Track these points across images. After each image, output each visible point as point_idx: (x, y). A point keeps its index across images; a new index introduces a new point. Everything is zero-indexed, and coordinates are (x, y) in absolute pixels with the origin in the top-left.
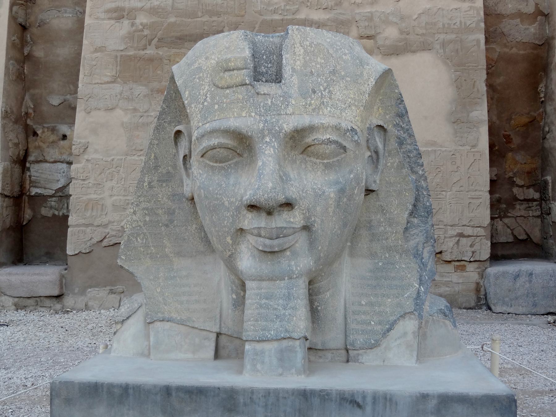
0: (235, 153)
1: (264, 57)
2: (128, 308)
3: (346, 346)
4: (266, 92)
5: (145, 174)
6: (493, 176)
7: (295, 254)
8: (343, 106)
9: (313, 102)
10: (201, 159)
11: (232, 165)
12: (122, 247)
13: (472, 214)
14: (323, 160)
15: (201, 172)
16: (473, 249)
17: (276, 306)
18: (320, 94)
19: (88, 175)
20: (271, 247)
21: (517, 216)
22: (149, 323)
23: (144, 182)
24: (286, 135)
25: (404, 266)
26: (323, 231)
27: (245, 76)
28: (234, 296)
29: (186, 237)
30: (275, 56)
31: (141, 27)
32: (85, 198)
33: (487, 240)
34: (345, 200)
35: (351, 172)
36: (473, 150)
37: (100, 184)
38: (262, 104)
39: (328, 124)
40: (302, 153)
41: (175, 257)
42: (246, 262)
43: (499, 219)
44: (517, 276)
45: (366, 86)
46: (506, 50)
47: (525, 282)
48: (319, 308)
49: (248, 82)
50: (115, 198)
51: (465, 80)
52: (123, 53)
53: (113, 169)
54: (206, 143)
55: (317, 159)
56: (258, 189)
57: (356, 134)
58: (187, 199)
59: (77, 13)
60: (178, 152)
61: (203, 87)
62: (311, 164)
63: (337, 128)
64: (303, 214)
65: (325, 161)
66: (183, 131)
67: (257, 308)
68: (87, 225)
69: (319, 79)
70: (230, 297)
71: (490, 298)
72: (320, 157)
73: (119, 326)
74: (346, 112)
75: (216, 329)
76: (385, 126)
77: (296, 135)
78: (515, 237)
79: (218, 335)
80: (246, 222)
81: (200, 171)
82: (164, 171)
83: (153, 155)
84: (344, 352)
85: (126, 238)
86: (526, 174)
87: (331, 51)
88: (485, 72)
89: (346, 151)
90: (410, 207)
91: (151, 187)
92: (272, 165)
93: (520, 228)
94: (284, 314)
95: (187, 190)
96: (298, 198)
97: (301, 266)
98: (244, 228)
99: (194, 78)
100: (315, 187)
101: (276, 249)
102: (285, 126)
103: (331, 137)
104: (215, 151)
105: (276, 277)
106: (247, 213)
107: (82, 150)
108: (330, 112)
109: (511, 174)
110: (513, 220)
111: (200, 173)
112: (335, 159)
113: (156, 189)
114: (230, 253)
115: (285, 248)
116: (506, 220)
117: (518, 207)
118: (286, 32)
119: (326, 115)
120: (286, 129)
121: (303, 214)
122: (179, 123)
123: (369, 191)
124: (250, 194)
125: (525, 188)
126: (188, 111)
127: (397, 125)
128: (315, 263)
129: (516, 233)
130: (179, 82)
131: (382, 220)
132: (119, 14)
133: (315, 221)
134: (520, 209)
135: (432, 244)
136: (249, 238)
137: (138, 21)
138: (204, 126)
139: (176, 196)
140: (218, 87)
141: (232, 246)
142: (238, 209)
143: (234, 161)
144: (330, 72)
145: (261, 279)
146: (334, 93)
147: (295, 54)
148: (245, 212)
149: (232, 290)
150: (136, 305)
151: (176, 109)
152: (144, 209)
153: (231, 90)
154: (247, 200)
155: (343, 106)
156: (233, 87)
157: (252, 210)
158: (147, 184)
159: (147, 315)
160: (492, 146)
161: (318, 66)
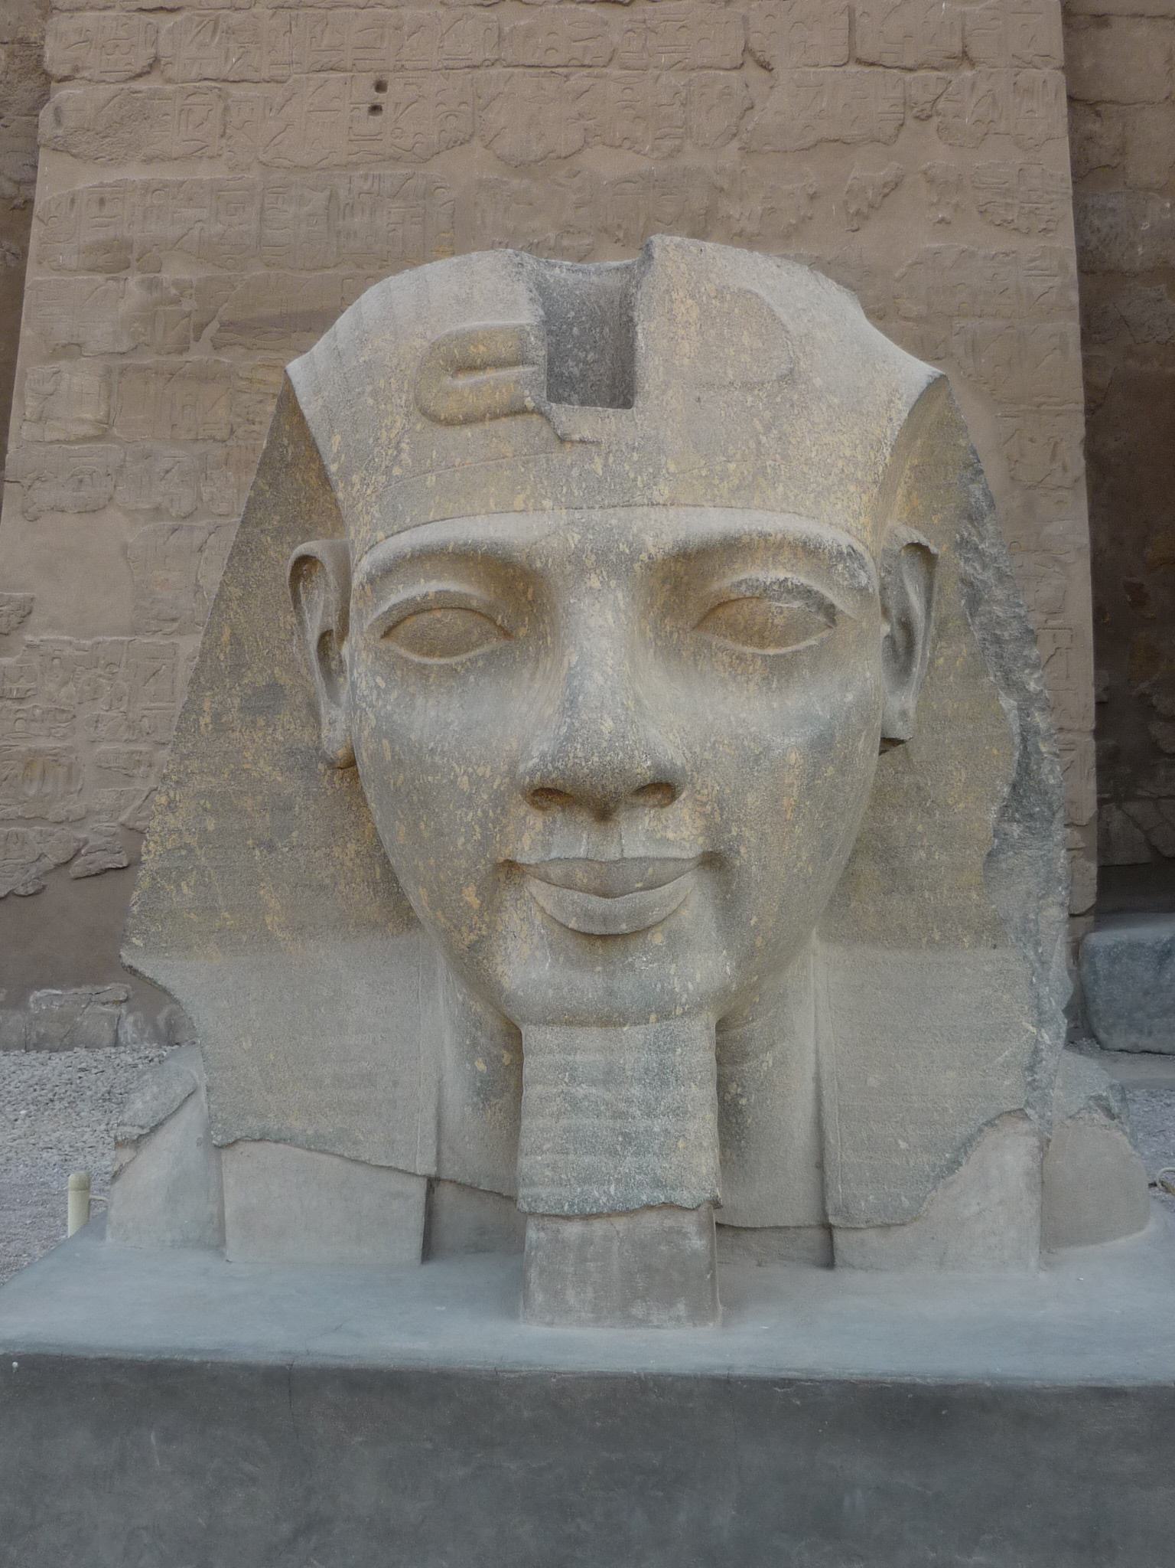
0: (488, 626)
1: (575, 330)
2: (155, 1098)
3: (825, 1214)
4: (587, 434)
7: (677, 943)
8: (820, 480)
9: (732, 466)
10: (383, 645)
11: (480, 664)
14: (762, 646)
15: (383, 685)
17: (622, 1106)
18: (752, 444)
19: (33, 685)
20: (605, 919)
23: (201, 712)
24: (650, 566)
26: (764, 867)
27: (523, 381)
28: (481, 1066)
29: (327, 881)
31: (173, 291)
32: (23, 747)
34: (831, 770)
36: (1052, 623)
37: (63, 711)
39: (780, 536)
40: (699, 625)
42: (527, 965)
45: (885, 422)
49: (530, 403)
50: (103, 747)
51: (1032, 440)
52: (126, 361)
53: (99, 671)
54: (399, 594)
55: (745, 643)
56: (569, 738)
57: (862, 567)
58: (331, 764)
59: (4, 257)
60: (301, 623)
61: (387, 421)
62: (726, 659)
63: (808, 550)
64: (703, 814)
65: (771, 651)
66: (319, 556)
68: (27, 821)
69: (750, 399)
73: (126, 1155)
75: (425, 1165)
76: (933, 549)
78: (1154, 849)
79: (433, 1183)
80: (526, 841)
81: (379, 680)
82: (261, 681)
83: (227, 631)
84: (817, 1235)
85: (146, 883)
87: (779, 311)
88: (1082, 419)
89: (833, 621)
90: (1006, 790)
91: (220, 726)
94: (648, 1131)
95: (334, 738)
97: (698, 976)
101: (624, 927)
102: (649, 540)
103: (789, 575)
104: (425, 618)
105: (621, 1014)
107: (14, 620)
108: (786, 497)
109: (1143, 686)
111: (378, 687)
114: (473, 937)
116: (1133, 808)
118: (639, 255)
120: (653, 551)
122: (307, 535)
123: (889, 743)
124: (543, 756)
126: (340, 495)
128: (739, 967)
130: (310, 407)
131: (920, 828)
132: (116, 258)
135: (1060, 899)
136: (534, 890)
137: (166, 276)
143: (486, 649)
144: (782, 378)
145: (572, 1018)
146: (793, 441)
147: (672, 320)
149: (475, 1043)
154: (532, 773)
155: (820, 480)
156: (481, 419)
157: (545, 804)
158: (208, 720)
159: (211, 1120)
160: (1099, 613)
161: (745, 358)
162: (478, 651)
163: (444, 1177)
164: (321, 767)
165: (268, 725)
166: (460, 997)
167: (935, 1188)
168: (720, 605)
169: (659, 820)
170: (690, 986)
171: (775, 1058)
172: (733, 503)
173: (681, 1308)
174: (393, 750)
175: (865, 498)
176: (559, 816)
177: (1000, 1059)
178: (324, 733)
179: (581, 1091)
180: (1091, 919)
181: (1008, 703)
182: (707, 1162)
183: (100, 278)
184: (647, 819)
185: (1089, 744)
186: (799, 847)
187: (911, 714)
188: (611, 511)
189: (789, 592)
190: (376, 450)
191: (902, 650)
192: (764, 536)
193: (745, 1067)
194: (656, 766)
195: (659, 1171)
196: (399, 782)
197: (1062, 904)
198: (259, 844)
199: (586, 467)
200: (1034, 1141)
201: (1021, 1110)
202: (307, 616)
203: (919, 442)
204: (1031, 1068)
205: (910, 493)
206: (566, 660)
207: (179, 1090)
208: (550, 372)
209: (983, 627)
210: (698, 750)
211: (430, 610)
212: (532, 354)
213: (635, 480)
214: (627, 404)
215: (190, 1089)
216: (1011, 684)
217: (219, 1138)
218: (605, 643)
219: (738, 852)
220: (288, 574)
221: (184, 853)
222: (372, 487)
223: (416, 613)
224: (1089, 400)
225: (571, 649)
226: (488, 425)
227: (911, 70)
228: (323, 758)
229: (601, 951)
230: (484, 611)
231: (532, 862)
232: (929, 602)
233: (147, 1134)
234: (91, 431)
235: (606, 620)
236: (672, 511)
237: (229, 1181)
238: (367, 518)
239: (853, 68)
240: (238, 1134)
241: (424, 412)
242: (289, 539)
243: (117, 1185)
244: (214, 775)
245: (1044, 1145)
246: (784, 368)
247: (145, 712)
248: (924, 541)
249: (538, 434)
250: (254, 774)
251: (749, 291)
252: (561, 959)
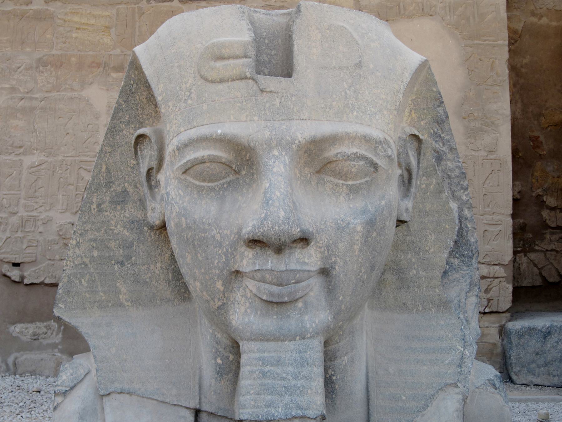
0: (229, 170)
1: (266, 41)
2: (72, 375)
4: (273, 89)
5: (93, 193)
6: (516, 193)
9: (334, 103)
10: (183, 177)
11: (225, 186)
12: (60, 291)
13: (488, 247)
14: (346, 180)
15: (182, 194)
16: (489, 296)
17: (284, 375)
18: (343, 93)
20: (279, 296)
21: (547, 250)
22: (102, 396)
23: (92, 203)
24: (300, 147)
25: (442, 323)
26: (346, 275)
27: (244, 65)
28: (219, 361)
29: (148, 280)
30: (280, 41)
33: (508, 283)
35: (382, 198)
38: (267, 105)
39: (354, 134)
40: (318, 172)
41: (133, 306)
42: (243, 315)
43: (522, 254)
44: (547, 333)
46: (534, 20)
47: (557, 342)
48: (334, 378)
49: (248, 75)
54: (191, 155)
55: (339, 179)
56: (265, 219)
57: (390, 147)
58: (152, 228)
60: (138, 164)
62: (331, 186)
63: (367, 139)
64: (320, 252)
65: (350, 183)
66: (148, 135)
67: (259, 378)
69: (342, 73)
70: (213, 361)
71: (511, 364)
72: (344, 178)
73: (59, 399)
74: (377, 117)
75: (193, 404)
76: (421, 137)
77: (312, 147)
78: (544, 278)
79: (197, 412)
80: (245, 262)
81: (180, 192)
82: (119, 189)
85: (65, 280)
86: (559, 192)
87: (355, 35)
88: (507, 49)
89: (377, 170)
90: (452, 244)
91: (100, 210)
92: (283, 187)
93: (550, 266)
94: (295, 386)
96: (314, 232)
98: (241, 270)
99: (172, 67)
100: (336, 217)
101: (286, 299)
102: (299, 136)
103: (358, 151)
104: (202, 166)
105: (284, 336)
106: (245, 250)
108: (357, 117)
109: (539, 191)
110: (541, 256)
112: (363, 181)
113: (108, 213)
114: (220, 303)
115: (298, 297)
116: (532, 256)
117: (548, 236)
118: (294, 9)
119: (351, 122)
120: (300, 139)
122: (142, 125)
123: (400, 222)
124: (254, 225)
125: (558, 211)
126: (163, 111)
127: (435, 135)
128: (334, 317)
129: (544, 274)
131: (413, 260)
133: (335, 262)
134: (551, 241)
135: (476, 293)
136: (247, 283)
138: (188, 131)
139: (137, 225)
140: (207, 80)
141: (224, 294)
142: (234, 245)
143: (228, 179)
145: (264, 337)
146: (361, 92)
148: (243, 249)
149: (217, 351)
150: (82, 371)
151: (137, 105)
152: (91, 240)
153: (225, 85)
154: (249, 233)
155: (372, 109)
156: (227, 81)
157: (254, 246)
162: (224, 180)
163: (202, 409)
164: (146, 228)
165: (122, 209)
166: (211, 331)
167: (417, 416)
168: (329, 163)
169: (302, 254)
170: (314, 325)
171: (348, 359)
172: (335, 119)
174: (186, 222)
175: (391, 116)
176: (259, 251)
177: (447, 362)
178: (149, 213)
179: (267, 368)
180: (508, 315)
181: (454, 206)
182: (320, 399)
184: (296, 254)
185: (510, 221)
186: (361, 267)
187: (410, 209)
188: (283, 122)
189: (358, 158)
190: (180, 92)
191: (407, 181)
192: (347, 134)
193: (336, 362)
194: (302, 231)
195: (300, 403)
196: (189, 236)
197: (477, 296)
198: (117, 263)
199: (273, 102)
200: (460, 397)
201: (455, 383)
202: (141, 161)
203: (415, 89)
204: (460, 366)
205: (411, 111)
206: (263, 185)
207: (82, 372)
208: (257, 61)
209: (443, 171)
210: (318, 224)
211: (205, 162)
212: (249, 54)
213: (293, 108)
214: (289, 75)
215: (86, 371)
216: (454, 197)
217: (103, 392)
218: (280, 179)
219: (335, 268)
220: (133, 142)
221: (83, 266)
222: (178, 108)
223: (198, 164)
224: (510, 38)
225: (266, 181)
226: (230, 83)
228: (148, 223)
229: (276, 309)
230: (227, 164)
231: (247, 271)
233: (69, 390)
235: (280, 168)
236: (309, 123)
237: (107, 410)
238: (176, 122)
240: (111, 390)
241: (202, 77)
242: (133, 126)
243: (57, 412)
244: (97, 231)
245: (465, 399)
246: (357, 61)
247: (5, 196)
248: (417, 133)
249: (252, 88)
250: (115, 231)
251: (343, 26)
252: (259, 313)
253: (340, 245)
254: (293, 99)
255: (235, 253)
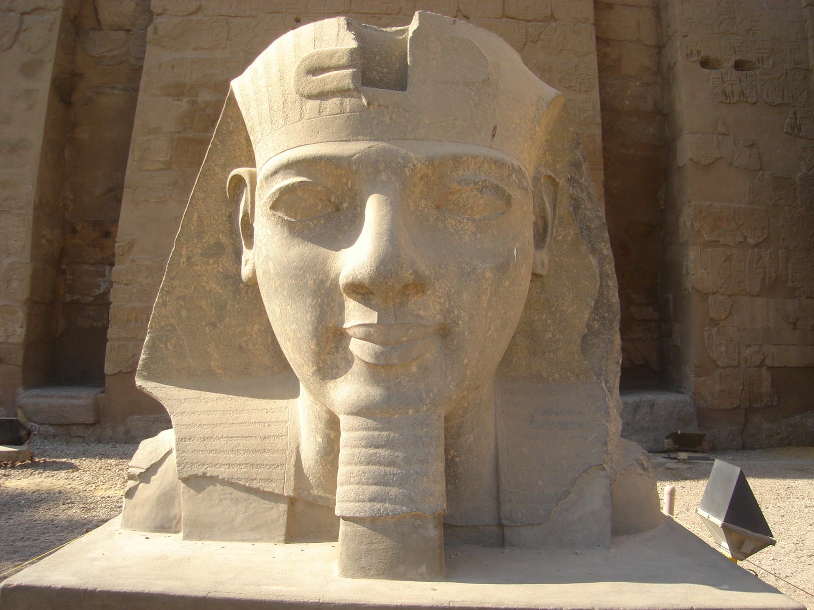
1: (378, 58)
3: (500, 519)
34: (507, 283)
48: (457, 459)
64: (440, 303)
82: (212, 241)
83: (196, 215)
88: (602, 172)
113: (199, 268)
121: (440, 303)
131: (549, 321)
144: (484, 81)
158: (184, 259)
165: (215, 263)
167: (557, 505)
173: (423, 569)
183: (170, 99)
187: (546, 262)
227: (529, 21)
232: (555, 206)
234: (163, 166)
239: (505, 20)
253: (465, 295)
254: (407, 115)
255: (333, 305)
